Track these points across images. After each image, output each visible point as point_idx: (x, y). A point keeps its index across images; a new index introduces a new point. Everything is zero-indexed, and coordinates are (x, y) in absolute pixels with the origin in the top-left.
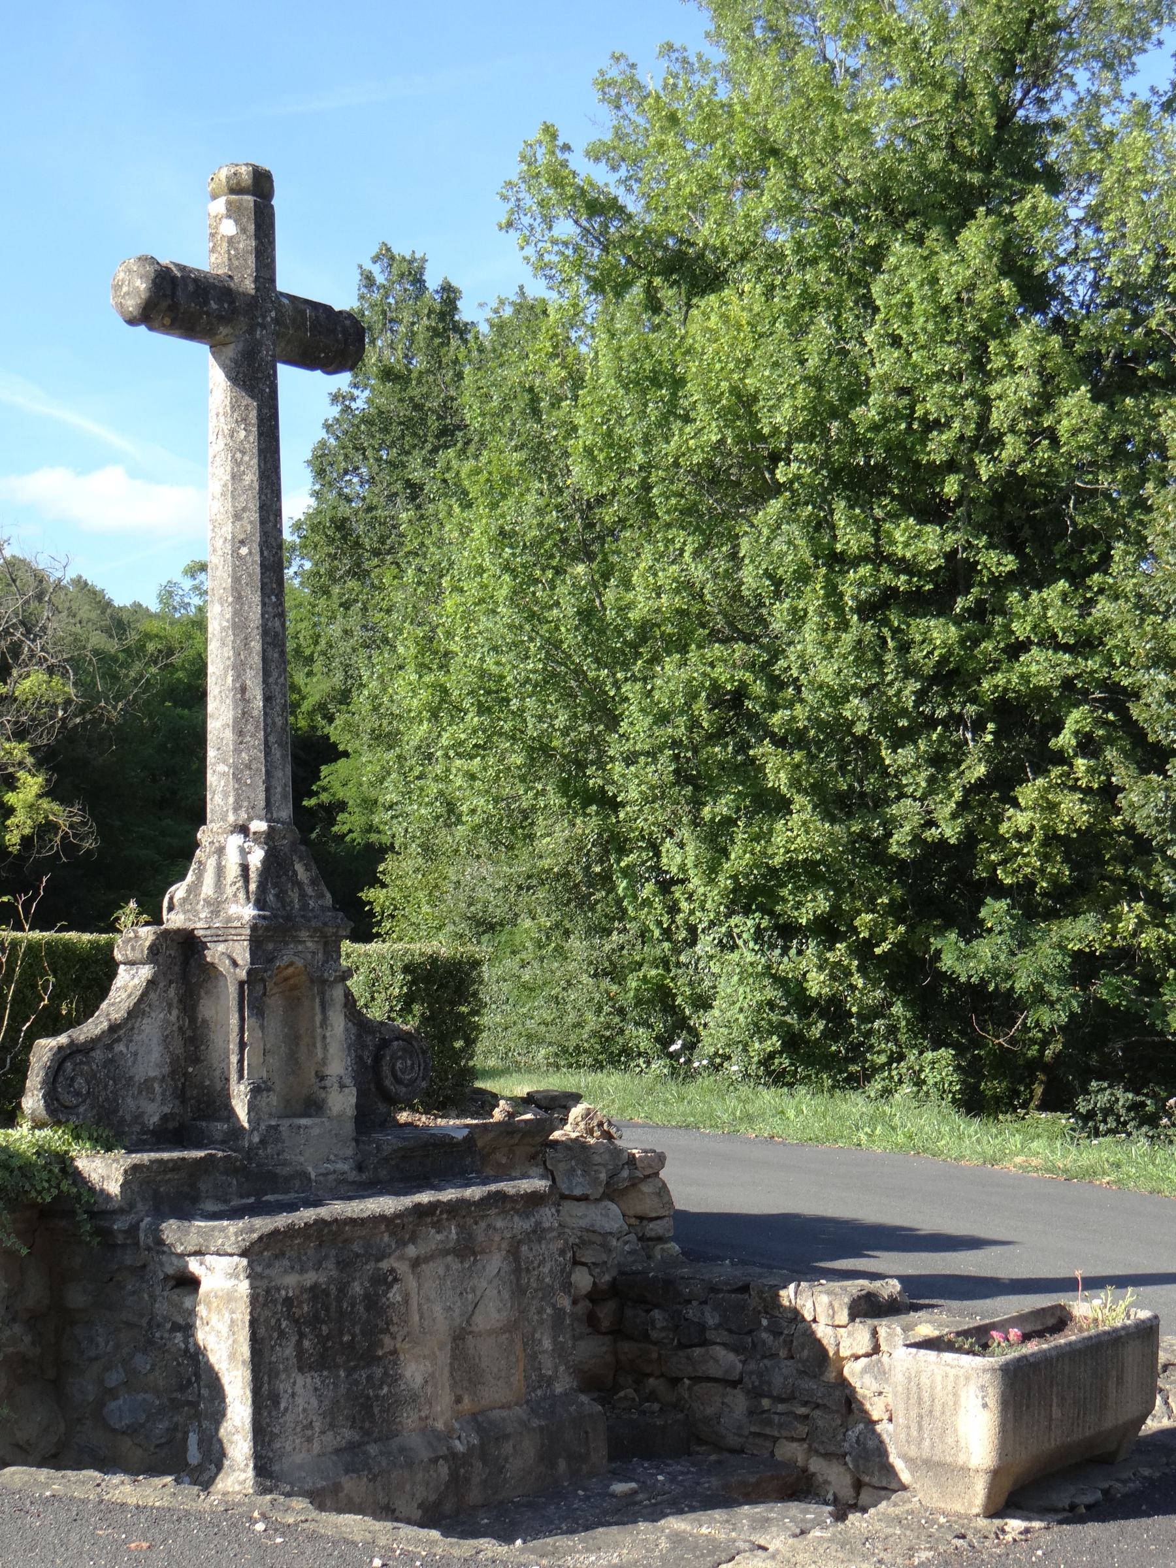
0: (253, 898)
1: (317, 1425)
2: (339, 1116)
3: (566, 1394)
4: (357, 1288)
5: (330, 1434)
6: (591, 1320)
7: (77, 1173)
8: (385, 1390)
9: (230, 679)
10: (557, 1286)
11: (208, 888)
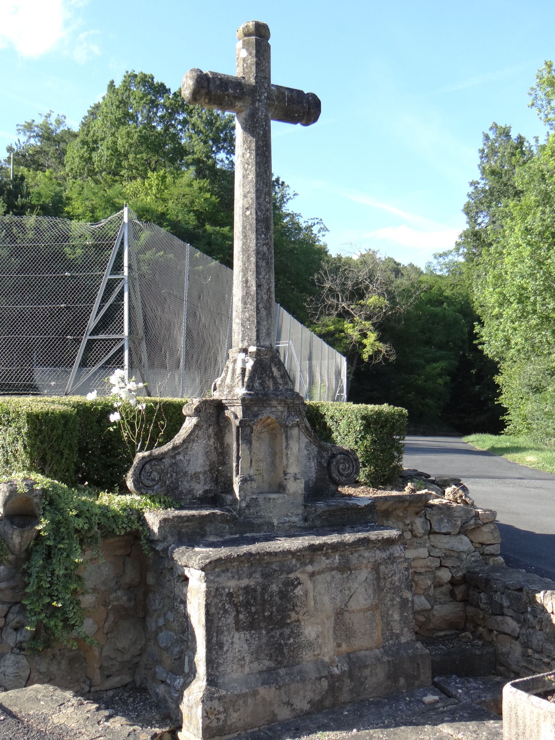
0: (245, 384)
1: (247, 659)
2: (294, 493)
3: (408, 643)
4: (274, 588)
5: (256, 663)
6: (452, 594)
7: (144, 520)
8: (292, 640)
9: (241, 276)
10: (403, 586)
11: (228, 381)
